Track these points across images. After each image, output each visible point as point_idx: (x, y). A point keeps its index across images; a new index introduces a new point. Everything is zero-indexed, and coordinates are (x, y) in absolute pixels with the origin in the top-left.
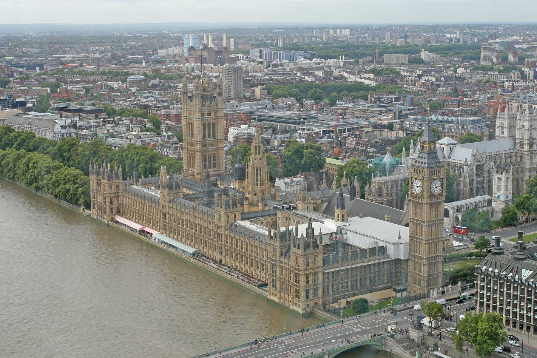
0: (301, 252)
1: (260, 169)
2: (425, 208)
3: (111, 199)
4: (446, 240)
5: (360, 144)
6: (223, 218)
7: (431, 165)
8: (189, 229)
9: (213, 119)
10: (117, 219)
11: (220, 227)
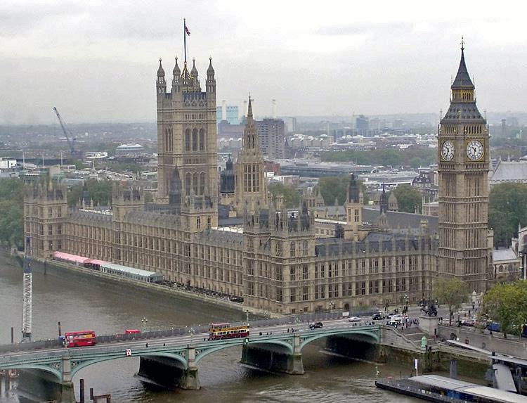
0: (285, 233)
1: (254, 168)
2: (461, 178)
3: (50, 227)
4: (515, 264)
5: (429, 190)
6: (193, 221)
7: (467, 120)
8: (148, 249)
9: (200, 124)
10: (56, 255)
11: (188, 235)
